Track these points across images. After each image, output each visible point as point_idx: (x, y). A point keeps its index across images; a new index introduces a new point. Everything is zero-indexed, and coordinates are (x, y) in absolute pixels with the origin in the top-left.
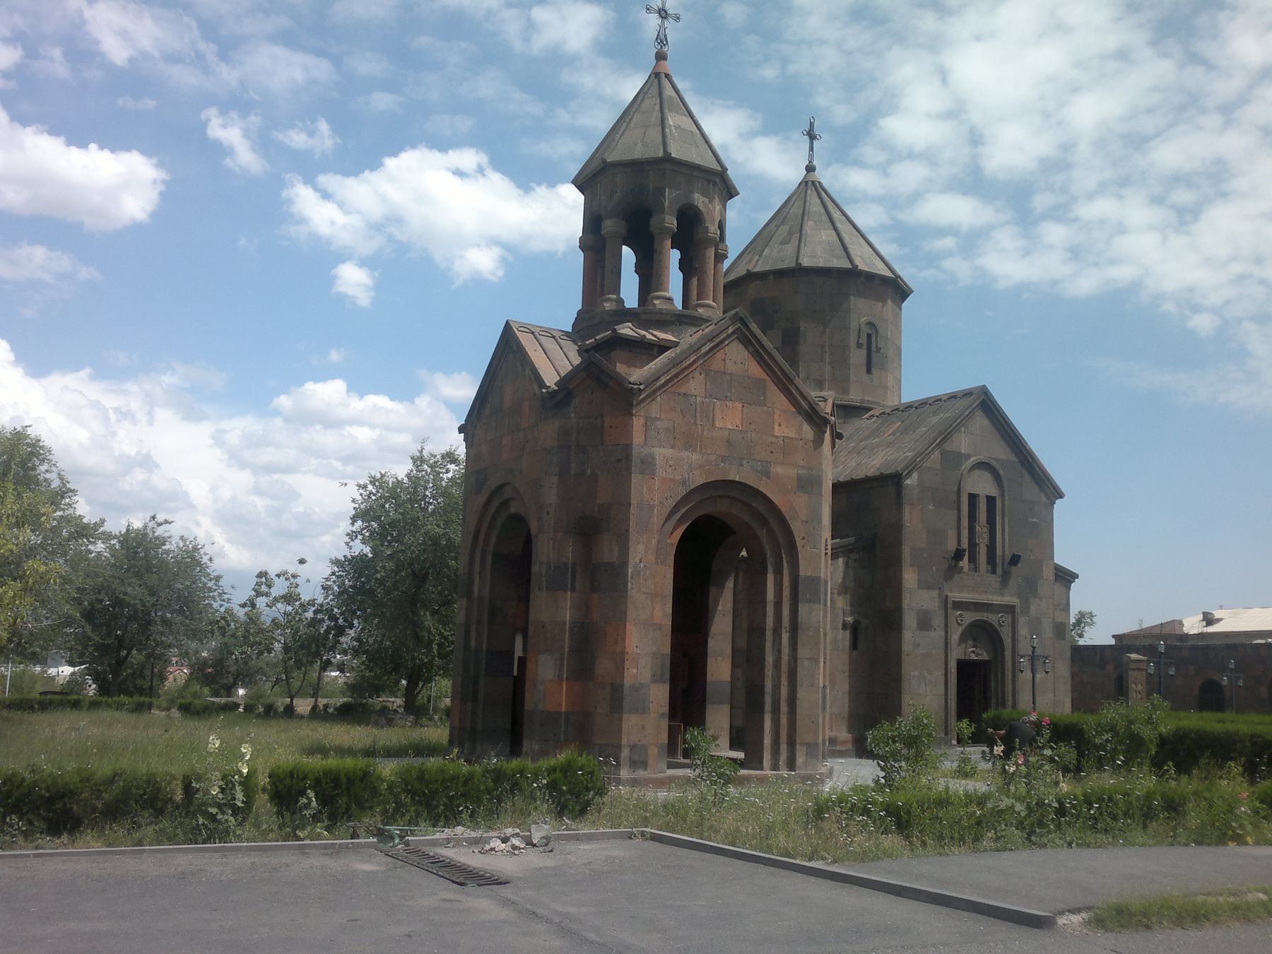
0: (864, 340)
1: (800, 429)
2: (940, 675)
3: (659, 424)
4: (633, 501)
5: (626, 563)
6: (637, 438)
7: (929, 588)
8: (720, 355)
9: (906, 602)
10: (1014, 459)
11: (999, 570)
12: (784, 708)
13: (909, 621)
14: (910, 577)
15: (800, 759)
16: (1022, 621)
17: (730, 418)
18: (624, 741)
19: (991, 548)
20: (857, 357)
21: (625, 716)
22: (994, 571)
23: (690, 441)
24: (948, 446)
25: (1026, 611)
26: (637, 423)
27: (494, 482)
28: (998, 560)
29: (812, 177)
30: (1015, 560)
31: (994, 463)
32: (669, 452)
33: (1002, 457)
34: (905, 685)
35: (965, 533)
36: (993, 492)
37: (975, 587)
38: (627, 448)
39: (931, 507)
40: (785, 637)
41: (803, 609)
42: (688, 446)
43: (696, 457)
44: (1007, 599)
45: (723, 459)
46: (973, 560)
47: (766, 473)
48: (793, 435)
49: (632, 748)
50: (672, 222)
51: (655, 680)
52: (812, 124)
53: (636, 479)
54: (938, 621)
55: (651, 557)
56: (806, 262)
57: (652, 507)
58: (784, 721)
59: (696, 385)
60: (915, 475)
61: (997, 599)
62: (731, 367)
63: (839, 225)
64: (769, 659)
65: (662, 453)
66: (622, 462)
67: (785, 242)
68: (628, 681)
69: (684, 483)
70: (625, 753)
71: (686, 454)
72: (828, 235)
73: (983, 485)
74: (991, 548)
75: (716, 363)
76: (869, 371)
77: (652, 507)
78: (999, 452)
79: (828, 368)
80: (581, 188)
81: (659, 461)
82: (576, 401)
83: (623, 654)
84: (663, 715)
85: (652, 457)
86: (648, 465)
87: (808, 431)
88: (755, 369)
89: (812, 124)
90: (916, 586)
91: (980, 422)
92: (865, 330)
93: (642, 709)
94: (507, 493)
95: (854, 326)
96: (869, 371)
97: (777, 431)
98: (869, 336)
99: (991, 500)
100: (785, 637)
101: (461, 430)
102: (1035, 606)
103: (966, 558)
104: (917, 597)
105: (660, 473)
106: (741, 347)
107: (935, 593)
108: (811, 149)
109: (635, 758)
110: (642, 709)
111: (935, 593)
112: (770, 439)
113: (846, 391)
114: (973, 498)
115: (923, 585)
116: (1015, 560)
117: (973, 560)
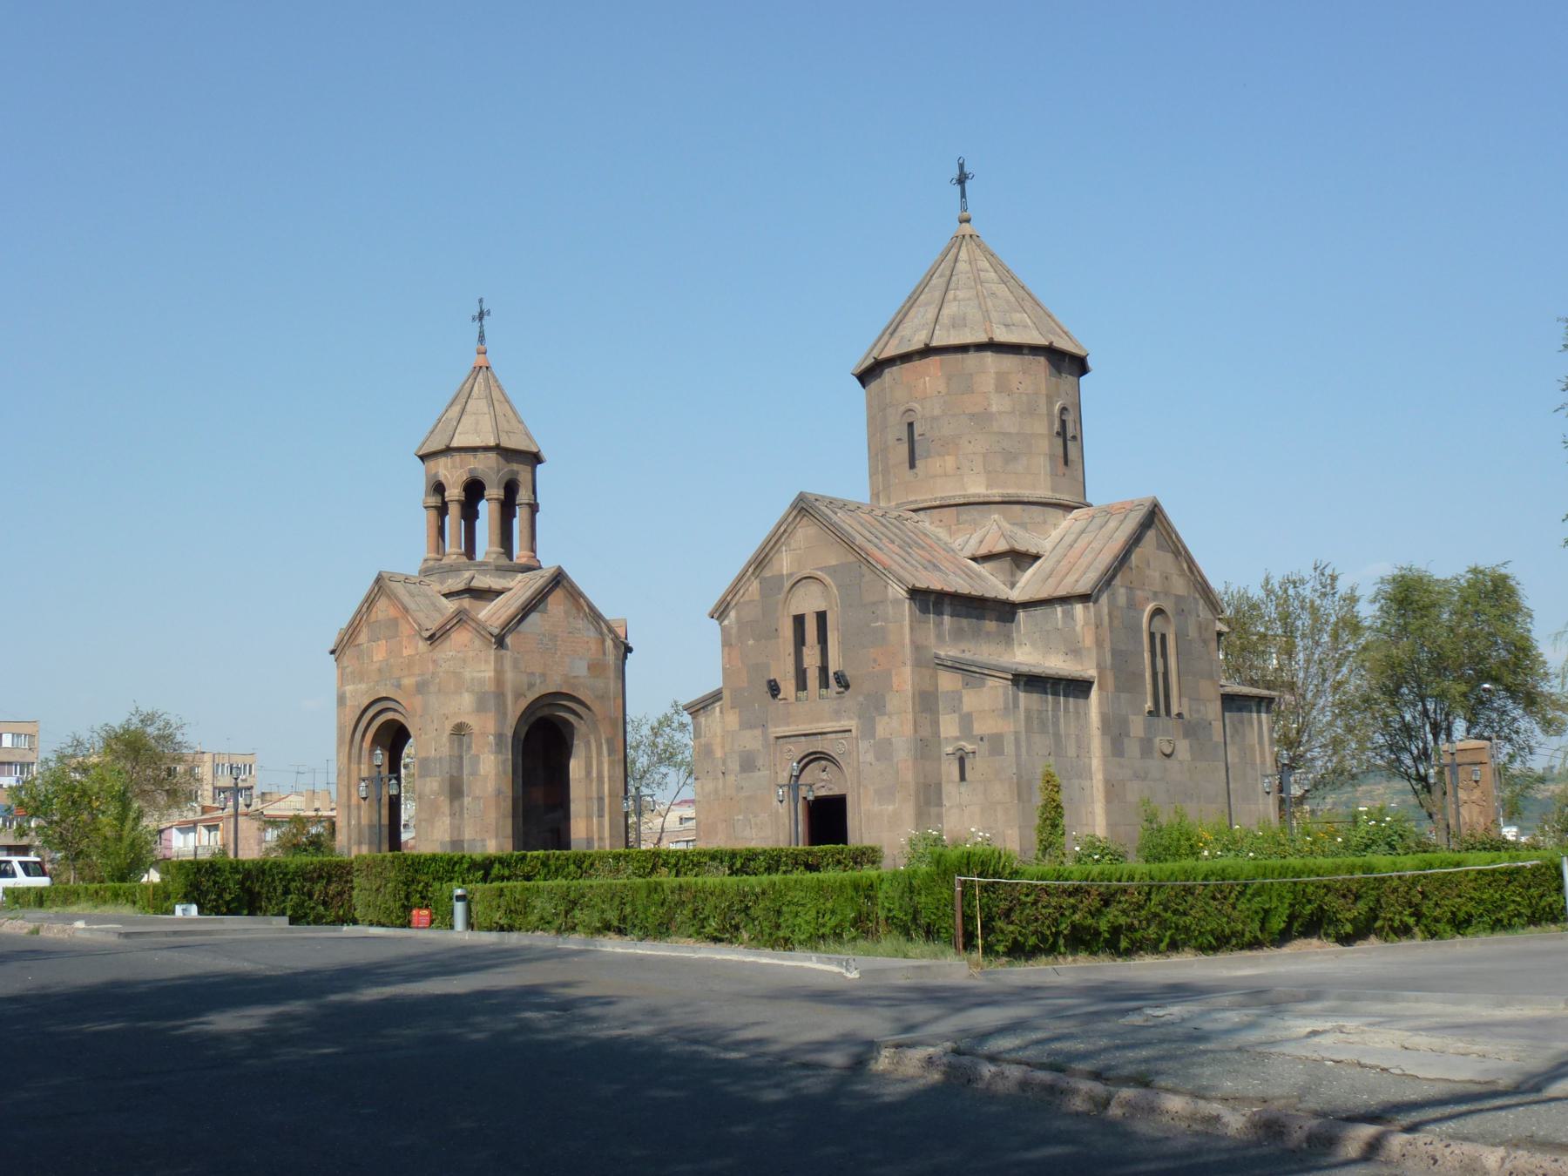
0: (905, 436)
7: (751, 727)
10: (851, 558)
17: (379, 653)
19: (824, 669)
24: (767, 573)
31: (819, 574)
33: (834, 563)
37: (816, 714)
39: (751, 642)
42: (361, 680)
43: (363, 686)
44: (845, 723)
46: (801, 684)
47: (399, 686)
52: (961, 166)
59: (363, 638)
60: (733, 614)
73: (808, 602)
74: (824, 669)
75: (373, 617)
76: (912, 465)
87: (423, 646)
88: (392, 612)
89: (961, 166)
90: (736, 727)
96: (912, 465)
97: (406, 653)
102: (883, 727)
111: (758, 732)
117: (801, 684)
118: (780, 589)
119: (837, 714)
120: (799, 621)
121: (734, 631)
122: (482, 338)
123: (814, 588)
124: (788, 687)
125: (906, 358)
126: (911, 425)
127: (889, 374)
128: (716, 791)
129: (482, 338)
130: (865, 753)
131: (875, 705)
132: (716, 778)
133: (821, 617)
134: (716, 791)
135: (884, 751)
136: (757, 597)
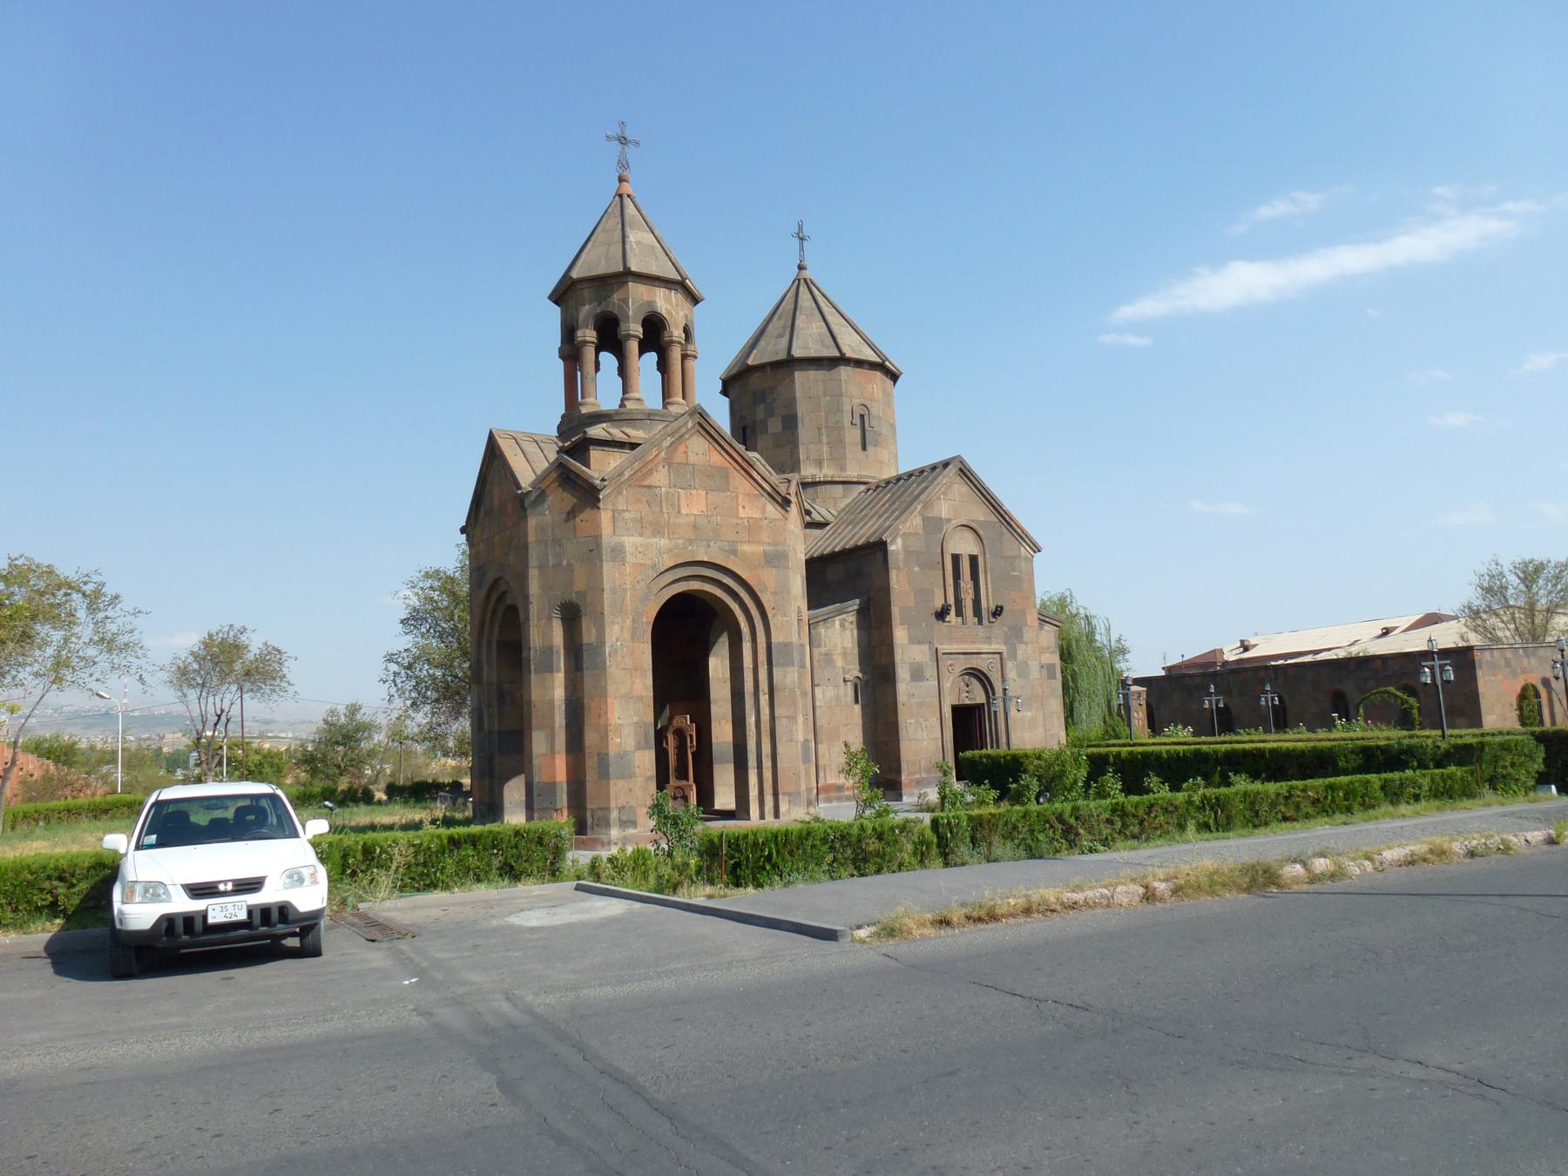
0: (857, 420)
1: (763, 510)
2: (935, 721)
3: (627, 515)
4: (607, 586)
5: (603, 643)
7: (920, 642)
8: (681, 449)
9: (898, 658)
11: (985, 621)
12: (767, 763)
13: (903, 674)
14: (900, 635)
15: (783, 808)
16: (1009, 665)
17: (694, 504)
18: (613, 804)
19: (977, 602)
20: (853, 435)
21: (612, 782)
22: (980, 622)
25: (1014, 656)
27: (491, 577)
28: (984, 613)
29: (807, 274)
30: (998, 612)
31: (974, 525)
32: (638, 540)
34: (902, 733)
35: (951, 590)
36: (975, 551)
38: (597, 539)
40: (764, 699)
41: (778, 673)
42: (657, 531)
43: (663, 542)
44: (994, 647)
45: (691, 542)
46: (959, 613)
47: (734, 552)
48: (757, 515)
49: (621, 809)
50: (637, 329)
51: (639, 747)
52: (800, 227)
53: (607, 567)
54: (930, 671)
55: (627, 635)
56: (797, 352)
57: (625, 590)
58: (768, 774)
60: (899, 541)
61: (985, 648)
62: (692, 459)
63: (829, 318)
65: (630, 542)
66: (593, 551)
67: (780, 336)
68: (612, 751)
69: (654, 567)
70: (614, 815)
71: (654, 540)
72: (818, 327)
73: (965, 545)
74: (977, 602)
75: (679, 457)
76: (864, 448)
77: (625, 590)
78: (980, 514)
79: (825, 448)
80: (556, 302)
81: (628, 548)
82: (550, 499)
83: (606, 725)
84: (649, 778)
85: (622, 545)
86: (618, 552)
87: (772, 510)
89: (800, 227)
91: (960, 489)
92: (858, 411)
93: (627, 774)
94: (502, 587)
95: (847, 408)
96: (864, 448)
97: (742, 513)
98: (862, 416)
99: (973, 560)
100: (764, 699)
101: (463, 530)
102: (1022, 651)
103: (953, 612)
104: (908, 651)
105: (630, 558)
106: (702, 440)
107: (925, 647)
108: (802, 248)
109: (625, 818)
110: (627, 774)
111: (925, 647)
112: (735, 521)
113: (843, 468)
114: (956, 559)
115: (914, 640)
116: (998, 612)
117: (959, 613)
118: (940, 529)
119: (988, 640)
120: (956, 559)
121: (901, 556)
122: (623, 164)
123: (969, 535)
124: (952, 617)
125: (859, 363)
126: (862, 416)
127: (845, 372)
128: (838, 697)
129: (623, 164)
130: (1011, 674)
131: (1015, 635)
132: (837, 686)
133: (973, 560)
134: (838, 697)
135: (1023, 671)
136: (921, 531)
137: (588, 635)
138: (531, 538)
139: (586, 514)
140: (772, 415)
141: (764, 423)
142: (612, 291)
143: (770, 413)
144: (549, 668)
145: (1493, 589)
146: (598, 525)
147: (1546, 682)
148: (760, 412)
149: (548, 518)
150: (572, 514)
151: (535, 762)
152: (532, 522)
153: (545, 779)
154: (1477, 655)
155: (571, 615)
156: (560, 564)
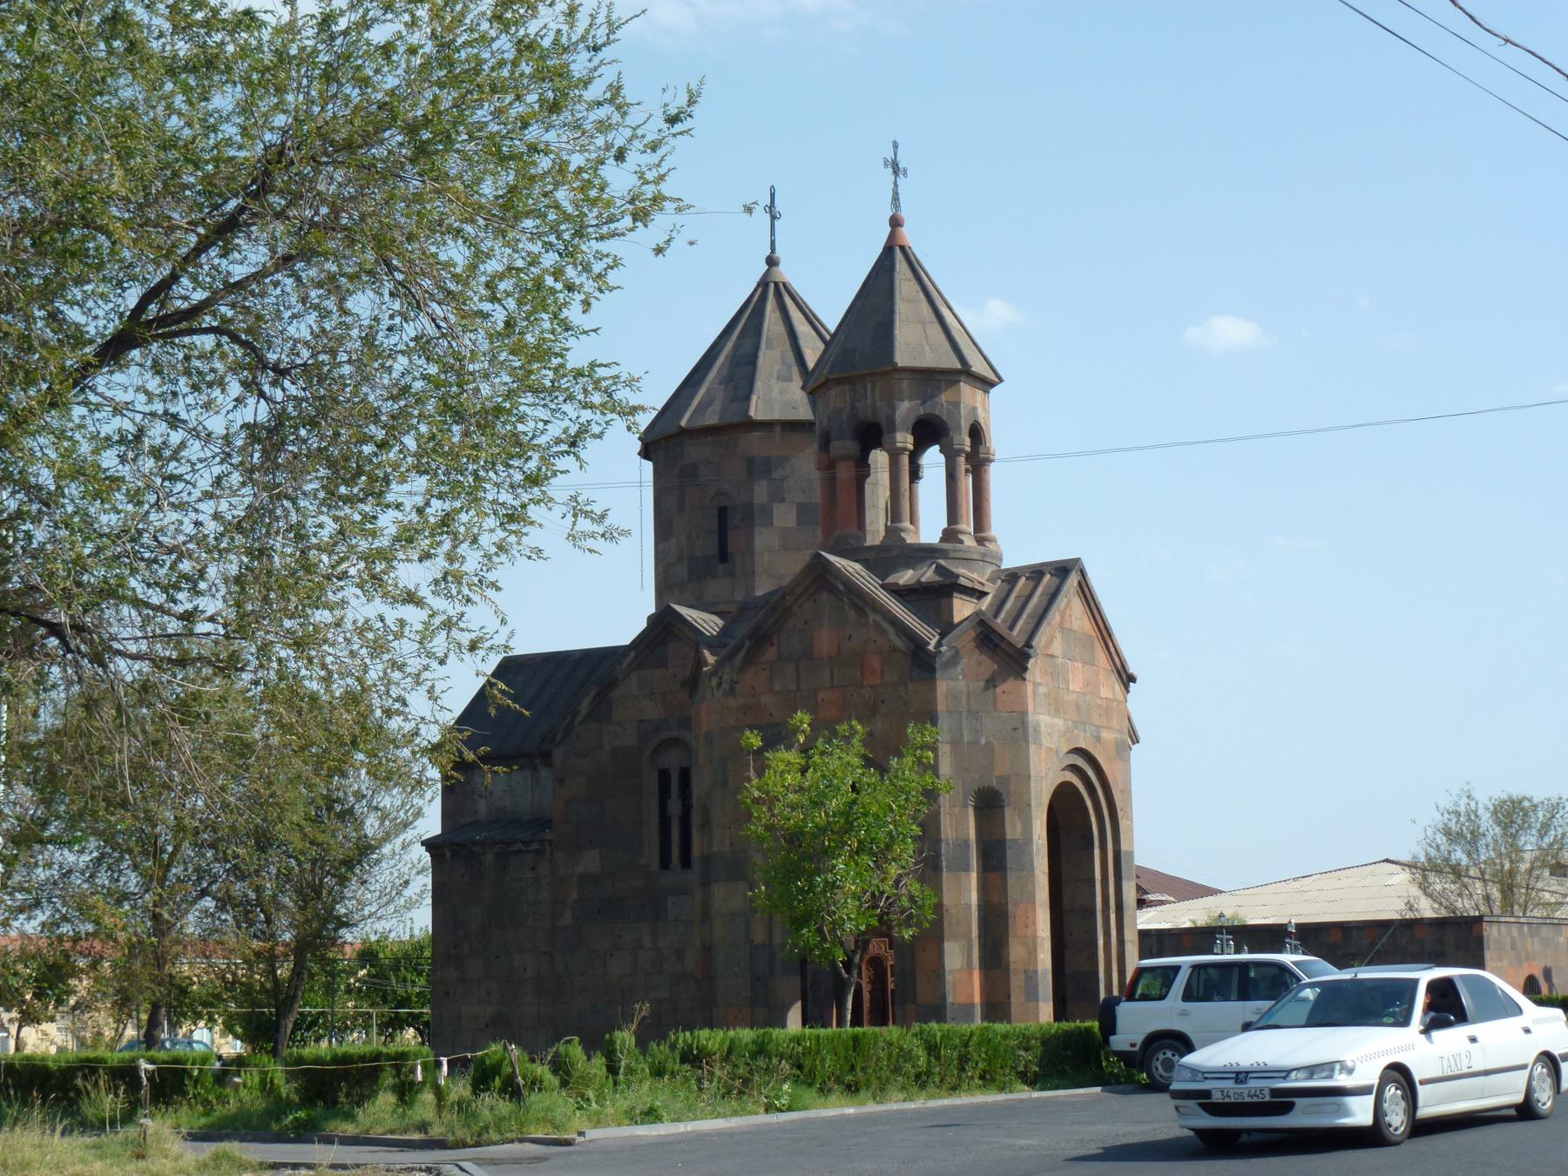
5: (1030, 840)
6: (1030, 709)
23: (1057, 707)
26: (1029, 688)
38: (1023, 715)
43: (1059, 723)
47: (1098, 739)
64: (1101, 942)
66: (1019, 731)
82: (965, 660)
86: (1037, 731)
87: (1118, 687)
122: (896, 198)
129: (896, 198)
137: (1013, 830)
138: (941, 707)
139: (1009, 685)
140: (782, 500)
141: (767, 512)
142: (939, 390)
143: (777, 496)
144: (967, 869)
145: (1462, 832)
146: (1023, 701)
147: (1547, 973)
148: (761, 492)
149: (961, 684)
150: (991, 682)
151: (949, 978)
152: (942, 687)
153: (962, 999)
154: (1491, 933)
155: (989, 804)
156: (977, 742)
